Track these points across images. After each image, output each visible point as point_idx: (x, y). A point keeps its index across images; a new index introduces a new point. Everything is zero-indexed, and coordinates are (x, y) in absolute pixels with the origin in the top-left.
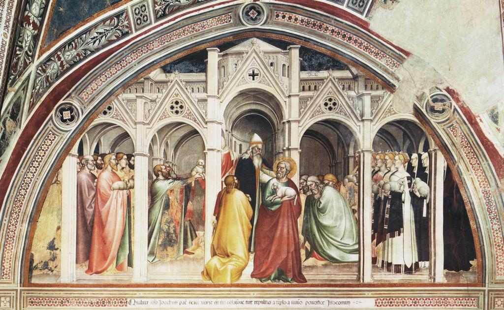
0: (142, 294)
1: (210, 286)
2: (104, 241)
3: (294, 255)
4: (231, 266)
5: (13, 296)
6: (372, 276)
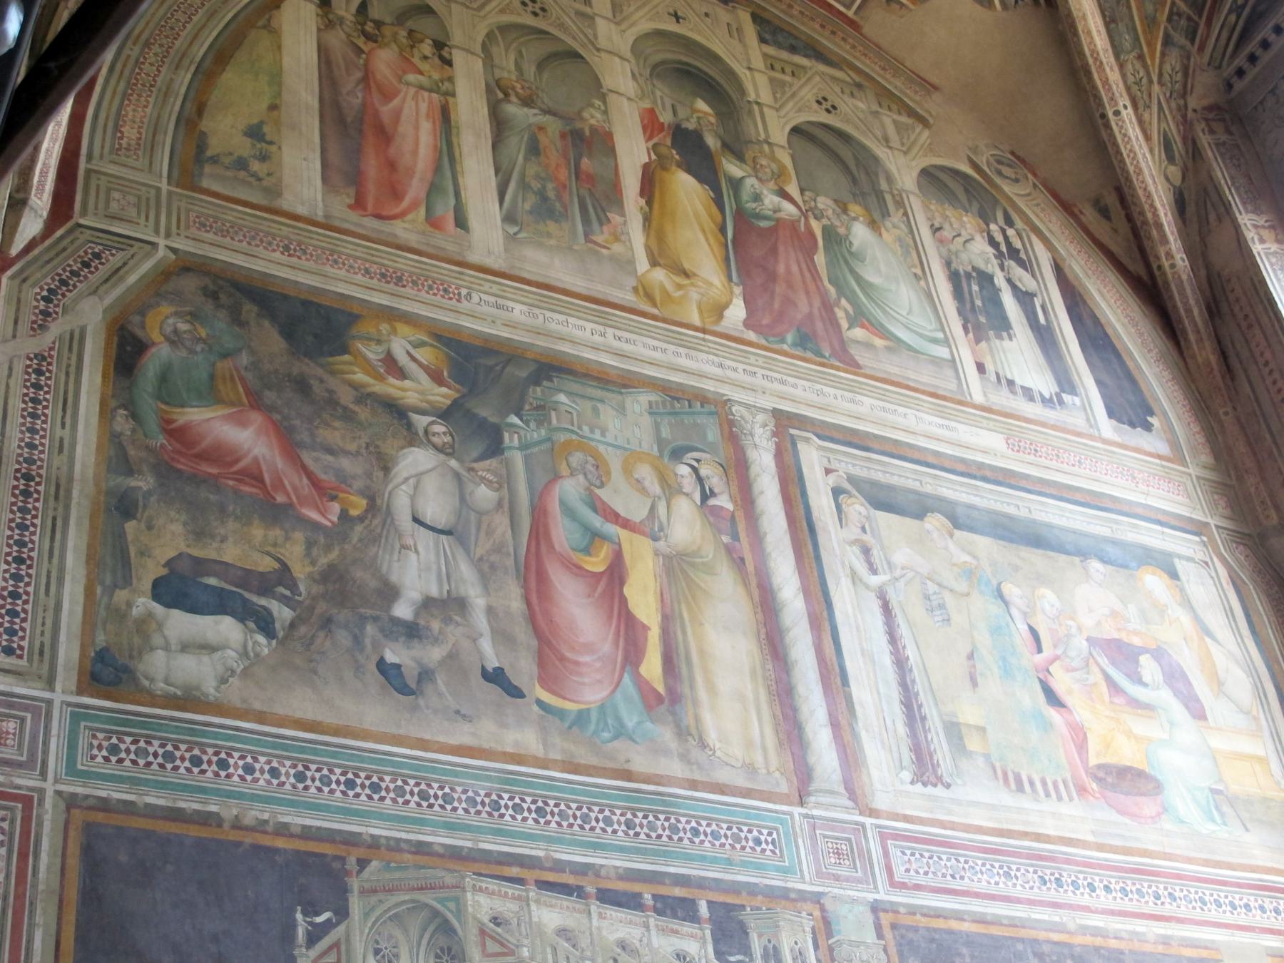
0: (495, 289)
1: (654, 318)
2: (392, 165)
5: (148, 199)
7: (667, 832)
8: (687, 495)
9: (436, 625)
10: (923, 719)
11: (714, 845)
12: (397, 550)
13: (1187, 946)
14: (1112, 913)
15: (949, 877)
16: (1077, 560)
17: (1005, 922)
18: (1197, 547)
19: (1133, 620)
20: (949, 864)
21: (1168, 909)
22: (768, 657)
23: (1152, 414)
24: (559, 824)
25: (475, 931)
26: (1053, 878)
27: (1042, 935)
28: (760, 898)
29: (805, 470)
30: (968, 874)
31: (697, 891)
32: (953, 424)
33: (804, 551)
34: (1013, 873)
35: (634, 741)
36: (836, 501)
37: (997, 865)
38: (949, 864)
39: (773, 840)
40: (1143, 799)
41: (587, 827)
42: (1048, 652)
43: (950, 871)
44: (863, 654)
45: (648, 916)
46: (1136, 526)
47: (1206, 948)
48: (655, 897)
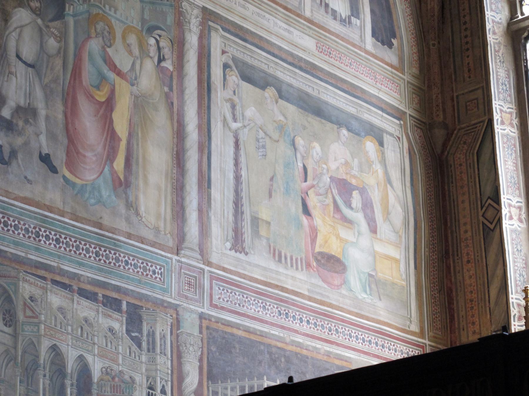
7: (114, 261)
8: (151, 58)
9: (21, 123)
10: (242, 213)
11: (134, 271)
12: (7, 74)
13: (338, 359)
14: (307, 335)
15: (237, 305)
16: (336, 127)
17: (258, 333)
18: (397, 128)
19: (355, 169)
20: (239, 298)
21: (333, 337)
22: (175, 166)
23: (394, 37)
24: (65, 249)
25: (22, 303)
26: (284, 313)
27: (274, 343)
28: (150, 303)
29: (212, 50)
30: (247, 305)
31: (123, 296)
32: (292, 29)
33: (203, 102)
34: (267, 307)
35: (105, 206)
36: (224, 72)
37: (260, 301)
38: (239, 298)
39: (161, 272)
40: (335, 275)
41: (78, 252)
42: (309, 183)
43: (239, 302)
44: (220, 170)
45: (99, 306)
46: (369, 110)
47: (346, 361)
48: (104, 296)
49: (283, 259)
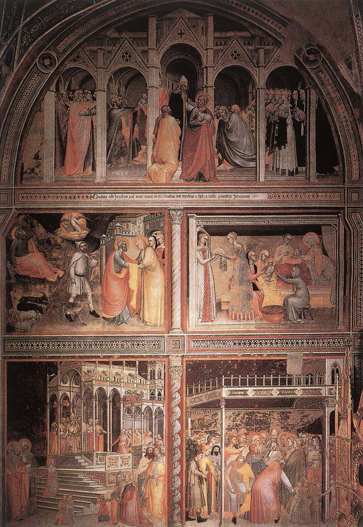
3: (210, 162)
4: (166, 169)
6: (265, 177)
9: (79, 302)
48: (126, 362)
49: (238, 318)
